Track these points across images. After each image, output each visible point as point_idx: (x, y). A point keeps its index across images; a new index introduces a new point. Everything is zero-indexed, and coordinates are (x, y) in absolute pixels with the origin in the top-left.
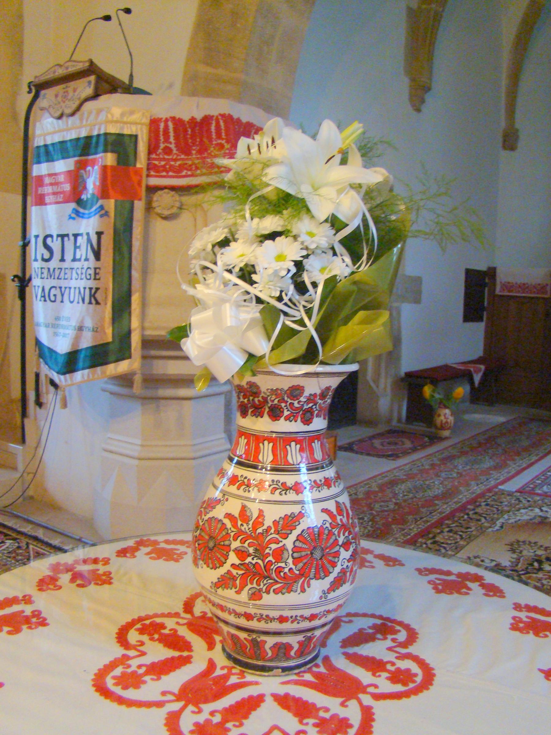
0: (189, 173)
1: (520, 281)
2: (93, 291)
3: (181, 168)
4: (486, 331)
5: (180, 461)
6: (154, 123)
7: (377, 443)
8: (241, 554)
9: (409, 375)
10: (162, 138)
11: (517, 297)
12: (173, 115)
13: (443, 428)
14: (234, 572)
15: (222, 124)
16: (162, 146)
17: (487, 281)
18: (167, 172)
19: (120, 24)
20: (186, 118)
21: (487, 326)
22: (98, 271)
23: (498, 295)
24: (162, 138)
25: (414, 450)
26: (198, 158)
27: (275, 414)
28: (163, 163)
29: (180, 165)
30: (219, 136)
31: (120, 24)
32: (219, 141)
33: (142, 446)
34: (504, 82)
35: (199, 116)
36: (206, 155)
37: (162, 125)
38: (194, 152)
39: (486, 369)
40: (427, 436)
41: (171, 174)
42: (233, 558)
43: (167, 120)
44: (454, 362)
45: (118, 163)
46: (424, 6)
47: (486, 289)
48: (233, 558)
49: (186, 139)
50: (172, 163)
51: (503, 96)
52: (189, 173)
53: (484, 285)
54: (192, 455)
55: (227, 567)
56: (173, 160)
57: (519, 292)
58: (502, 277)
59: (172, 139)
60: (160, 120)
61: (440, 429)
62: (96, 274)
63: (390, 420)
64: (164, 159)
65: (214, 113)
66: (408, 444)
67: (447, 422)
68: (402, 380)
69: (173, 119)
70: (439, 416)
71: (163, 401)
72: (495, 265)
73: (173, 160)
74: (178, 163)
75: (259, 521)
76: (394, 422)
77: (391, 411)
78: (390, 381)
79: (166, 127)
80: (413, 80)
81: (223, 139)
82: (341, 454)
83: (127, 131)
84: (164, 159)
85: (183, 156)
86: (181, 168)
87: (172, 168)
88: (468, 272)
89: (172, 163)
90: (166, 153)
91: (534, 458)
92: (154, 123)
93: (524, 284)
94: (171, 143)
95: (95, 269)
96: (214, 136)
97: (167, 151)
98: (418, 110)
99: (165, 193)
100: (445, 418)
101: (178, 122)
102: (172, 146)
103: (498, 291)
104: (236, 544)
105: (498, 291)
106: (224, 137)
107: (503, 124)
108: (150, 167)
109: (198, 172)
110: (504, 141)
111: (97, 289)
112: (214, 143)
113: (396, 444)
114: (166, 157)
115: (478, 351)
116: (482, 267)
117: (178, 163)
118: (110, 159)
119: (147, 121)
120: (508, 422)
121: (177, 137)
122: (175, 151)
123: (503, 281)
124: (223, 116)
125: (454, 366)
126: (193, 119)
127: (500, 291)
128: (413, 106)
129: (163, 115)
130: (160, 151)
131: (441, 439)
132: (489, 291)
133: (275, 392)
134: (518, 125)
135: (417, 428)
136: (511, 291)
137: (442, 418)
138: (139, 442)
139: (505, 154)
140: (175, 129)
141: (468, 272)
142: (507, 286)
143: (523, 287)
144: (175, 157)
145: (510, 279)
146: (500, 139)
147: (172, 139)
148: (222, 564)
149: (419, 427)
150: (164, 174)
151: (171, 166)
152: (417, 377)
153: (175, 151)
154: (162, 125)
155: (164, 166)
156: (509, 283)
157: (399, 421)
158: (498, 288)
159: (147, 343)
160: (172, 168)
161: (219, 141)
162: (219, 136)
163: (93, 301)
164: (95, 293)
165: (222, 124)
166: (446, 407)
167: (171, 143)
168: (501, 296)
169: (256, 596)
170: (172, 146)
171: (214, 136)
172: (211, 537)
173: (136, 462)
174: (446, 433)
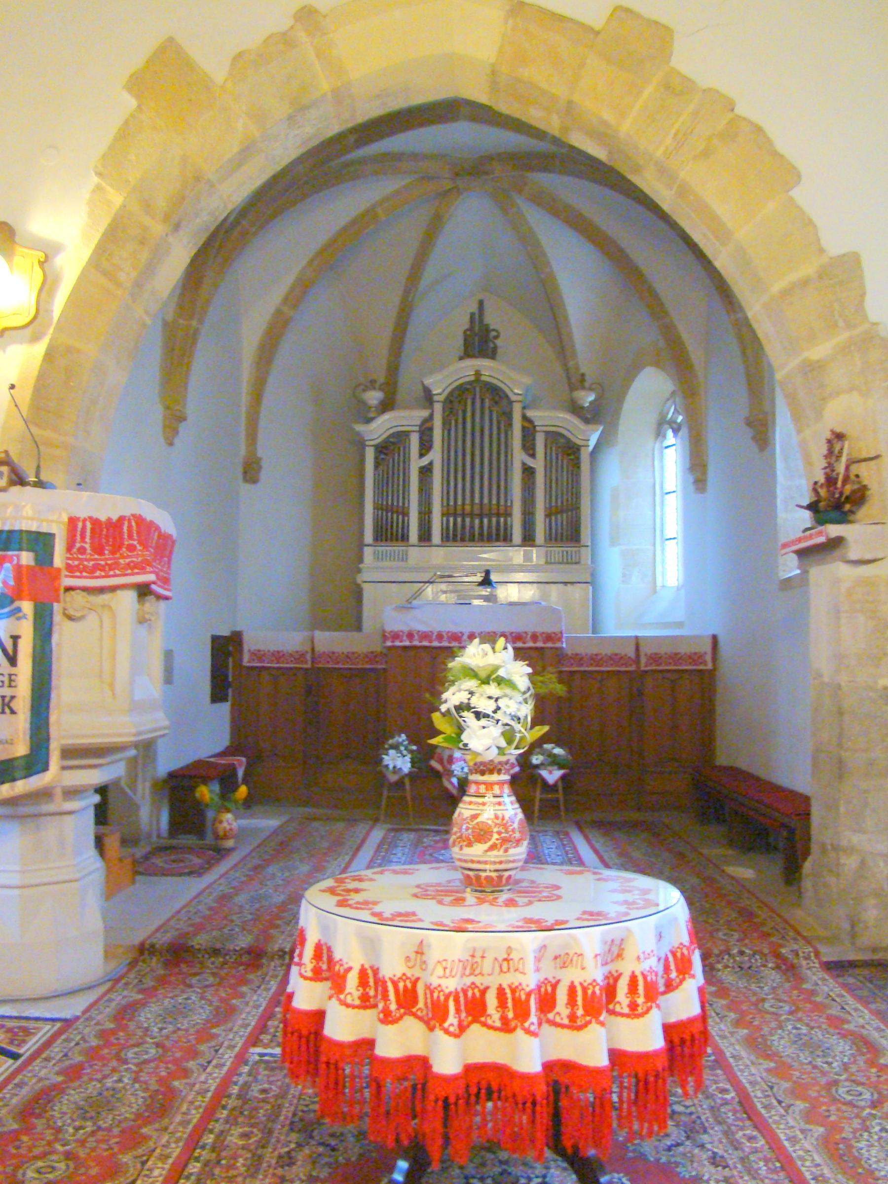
0: (103, 574)
1: (273, 648)
2: (7, 700)
3: (96, 567)
4: (232, 712)
5: (46, 887)
6: (72, 521)
7: (159, 861)
8: (499, 833)
9: (172, 775)
10: (78, 538)
11: (270, 667)
12: (90, 515)
13: (226, 837)
14: (497, 842)
15: (134, 524)
16: (78, 545)
17: (231, 648)
18: (81, 572)
19: (16, 406)
20: (103, 518)
21: (232, 705)
22: (13, 677)
23: (245, 667)
24: (78, 538)
25: (209, 865)
26: (111, 559)
27: (499, 772)
28: (76, 563)
29: (94, 565)
30: (130, 537)
31: (16, 406)
32: (131, 542)
33: (23, 872)
34: (245, 400)
35: (115, 518)
36: (118, 555)
37: (80, 525)
38: (106, 552)
39: (248, 763)
40: (210, 849)
41: (85, 574)
42: (496, 836)
43: (84, 521)
44: (211, 753)
45: (36, 564)
46: (181, 321)
47: (231, 660)
48: (496, 836)
49: (100, 538)
50: (86, 563)
51: (243, 415)
52: (103, 574)
53: (230, 654)
54: (78, 875)
55: (493, 840)
56: (86, 560)
57: (272, 662)
58: (250, 643)
59: (88, 539)
60: (78, 519)
61: (222, 839)
62: (11, 680)
63: (149, 835)
64: (78, 559)
65: (127, 513)
66: (197, 861)
67: (231, 829)
68: (165, 781)
69: (91, 518)
70: (221, 822)
71: (42, 819)
72: (238, 629)
73: (86, 560)
74: (92, 563)
75: (503, 819)
76: (154, 839)
77: (151, 824)
78: (148, 784)
79: (84, 527)
80: (167, 408)
81: (134, 540)
82: (139, 878)
83: (45, 529)
84: (78, 559)
85: (96, 556)
86: (96, 567)
87: (85, 569)
88: (215, 639)
89: (86, 563)
90: (82, 554)
91: (347, 858)
92: (72, 521)
93: (278, 652)
94: (86, 543)
95: (10, 675)
96: (126, 536)
97: (82, 550)
98: (171, 444)
99: (77, 594)
100: (229, 824)
101: (95, 522)
102: (87, 546)
103: (246, 661)
104: (495, 830)
105: (246, 660)
106: (135, 537)
107: (243, 451)
108: (69, 568)
109: (112, 573)
110: (245, 473)
111: (13, 697)
112: (126, 543)
113: (182, 861)
114: (80, 556)
115: (223, 740)
116: (226, 632)
117: (92, 563)
118: (26, 558)
119: (65, 519)
120: (281, 827)
121: (92, 538)
122: (89, 551)
123: (252, 649)
124: (133, 515)
125: (212, 760)
126: (109, 519)
127: (249, 662)
128: (166, 439)
129: (83, 515)
130: (75, 550)
131: (230, 850)
132: (234, 662)
133: (500, 763)
134: (260, 453)
135: (184, 842)
136: (263, 661)
137: (225, 825)
138: (17, 868)
139: (246, 488)
140: (93, 530)
141: (215, 639)
142: (257, 655)
143: (278, 656)
144: (88, 557)
145: (262, 647)
146: (240, 469)
147: (88, 539)
148: (490, 840)
149: (189, 840)
150: (78, 574)
151: (84, 565)
152: (184, 776)
153: (89, 551)
154: (80, 525)
155: (77, 566)
156: (259, 651)
157: (159, 836)
158: (246, 658)
159: (68, 753)
160: (85, 569)
161: (131, 542)
162: (130, 537)
163: (7, 710)
164: (10, 701)
165: (134, 524)
166: (228, 811)
167: (86, 543)
168: (252, 668)
169: (506, 851)
170: (87, 546)
171: (126, 536)
172: (481, 830)
173: (17, 892)
174: (230, 843)
